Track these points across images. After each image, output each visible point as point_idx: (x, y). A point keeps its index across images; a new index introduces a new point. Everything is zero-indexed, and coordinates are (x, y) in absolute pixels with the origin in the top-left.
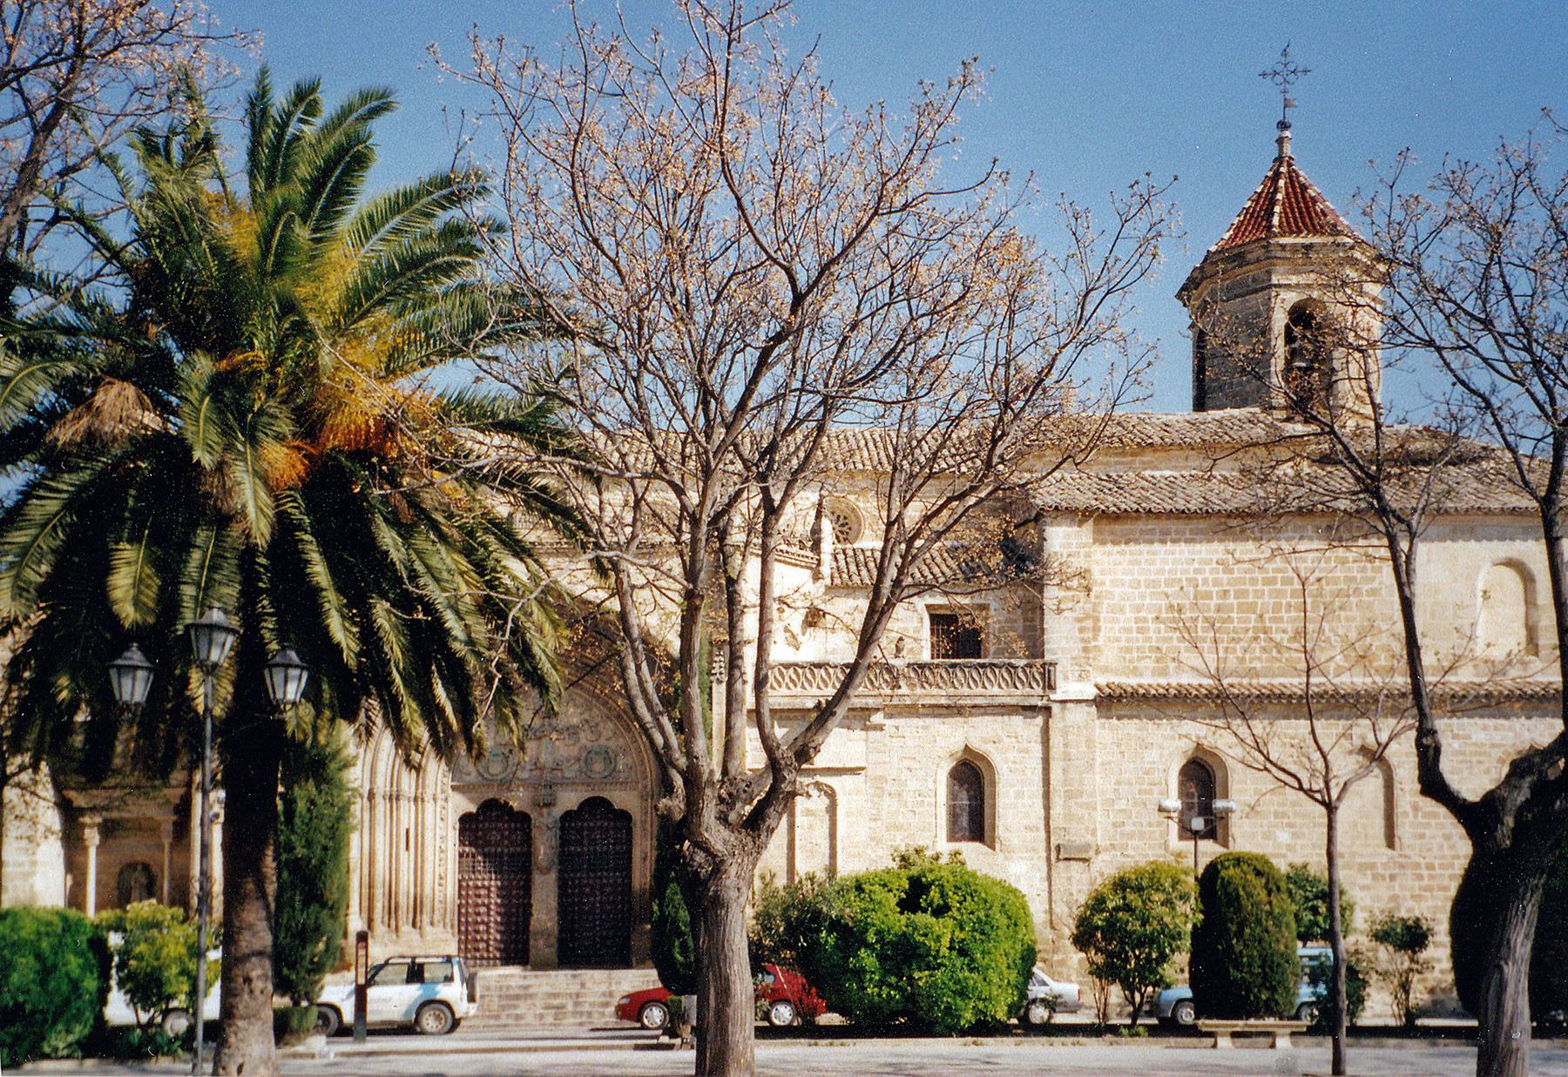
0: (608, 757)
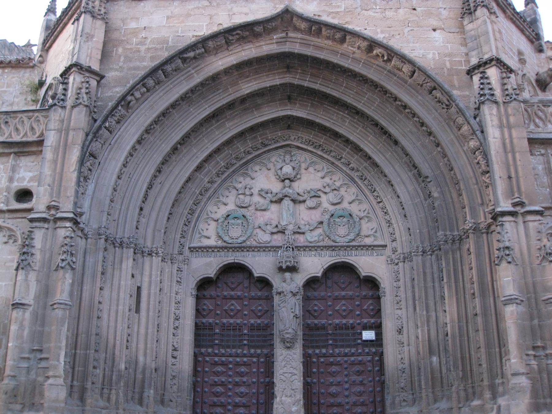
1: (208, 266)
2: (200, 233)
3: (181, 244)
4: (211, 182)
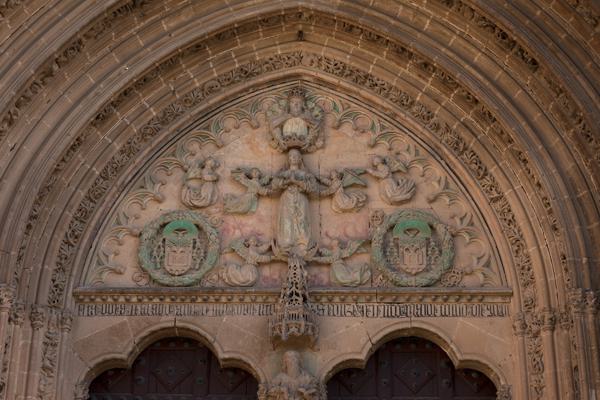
0: (433, 238)
1: (116, 334)
2: (99, 263)
3: (56, 286)
4: (129, 151)
